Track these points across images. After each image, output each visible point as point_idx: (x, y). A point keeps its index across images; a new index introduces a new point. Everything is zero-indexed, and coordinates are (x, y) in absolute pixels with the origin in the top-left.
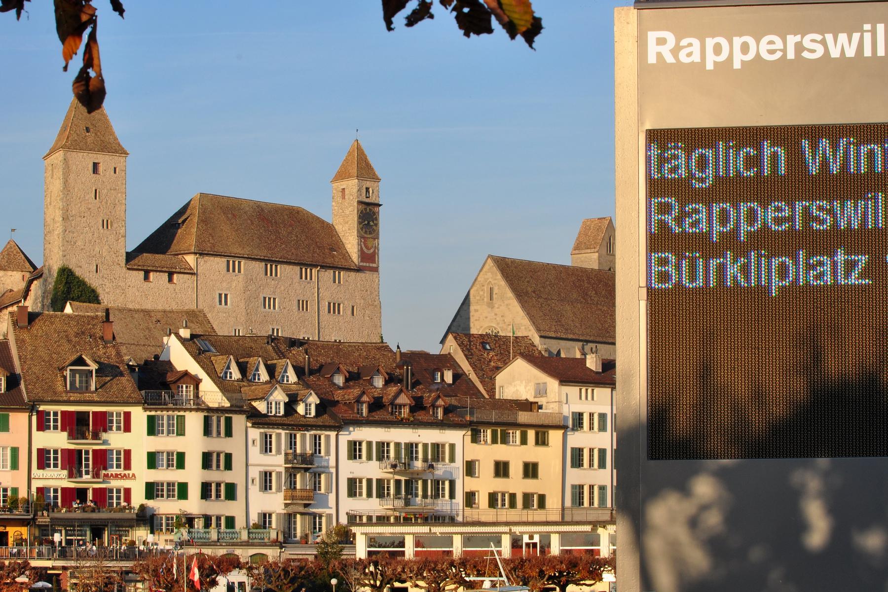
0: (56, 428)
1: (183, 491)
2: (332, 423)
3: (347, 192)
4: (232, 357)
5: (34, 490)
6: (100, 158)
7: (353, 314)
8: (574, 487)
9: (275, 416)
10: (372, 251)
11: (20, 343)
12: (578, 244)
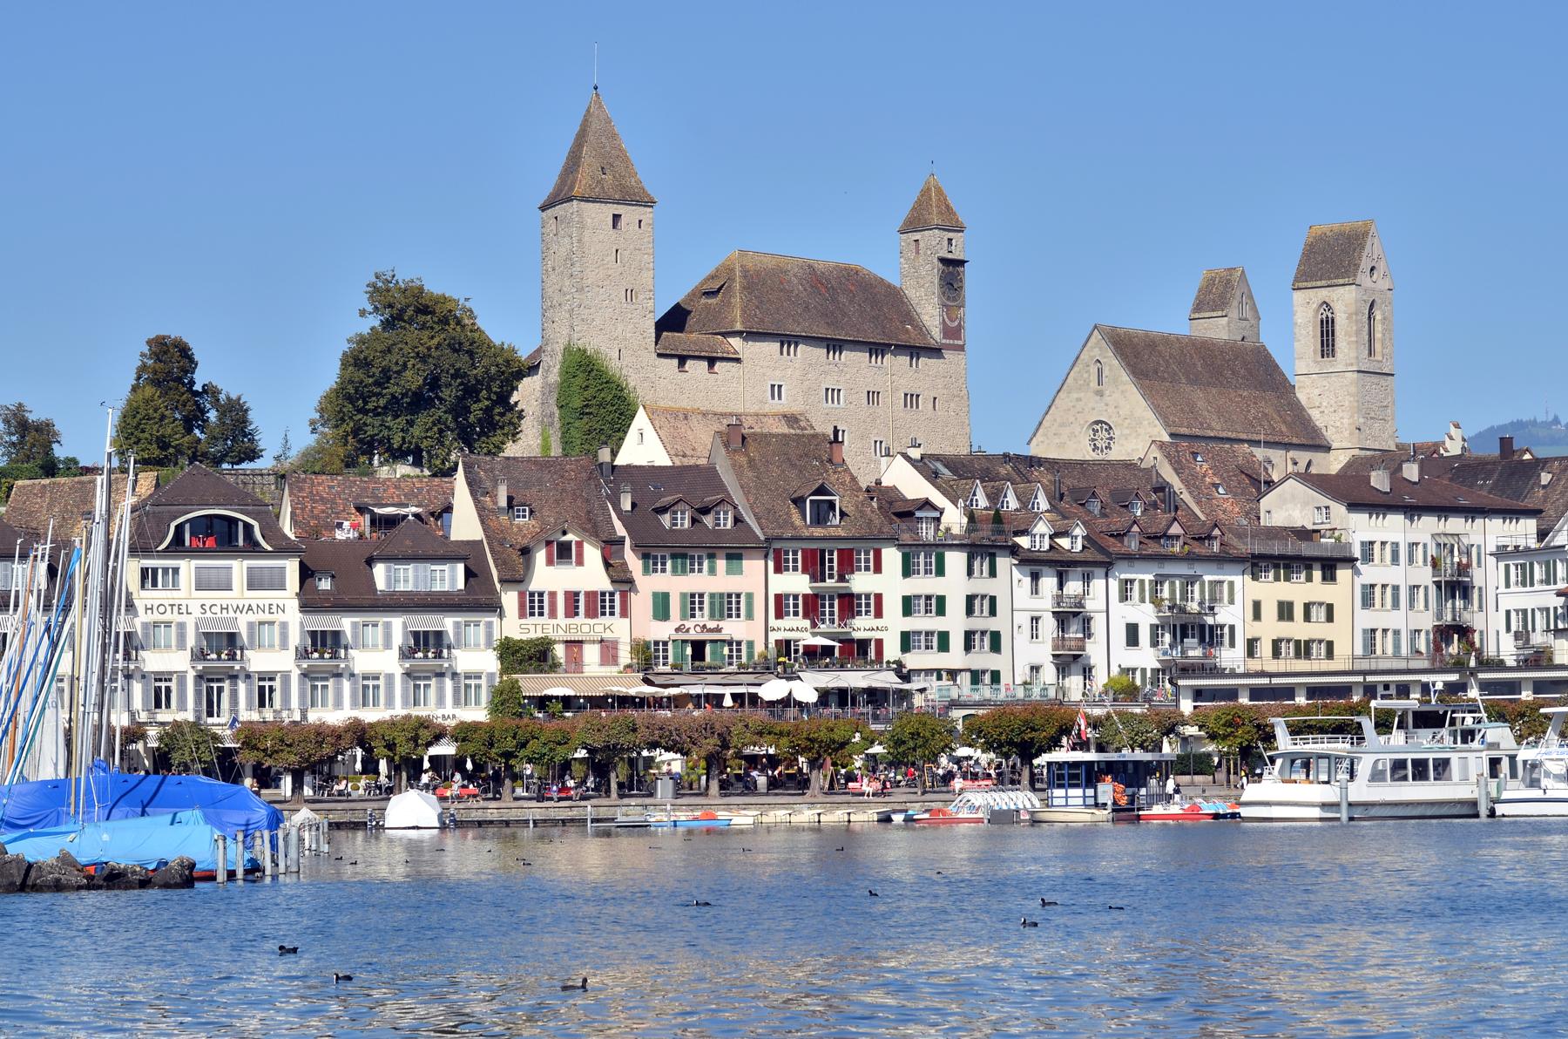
0: (795, 569)
1: (944, 642)
2: (1100, 558)
3: (922, 244)
4: (978, 481)
5: (772, 645)
6: (619, 209)
7: (934, 407)
8: (1365, 631)
9: (1039, 551)
10: (956, 323)
11: (737, 468)
12: (1198, 304)
